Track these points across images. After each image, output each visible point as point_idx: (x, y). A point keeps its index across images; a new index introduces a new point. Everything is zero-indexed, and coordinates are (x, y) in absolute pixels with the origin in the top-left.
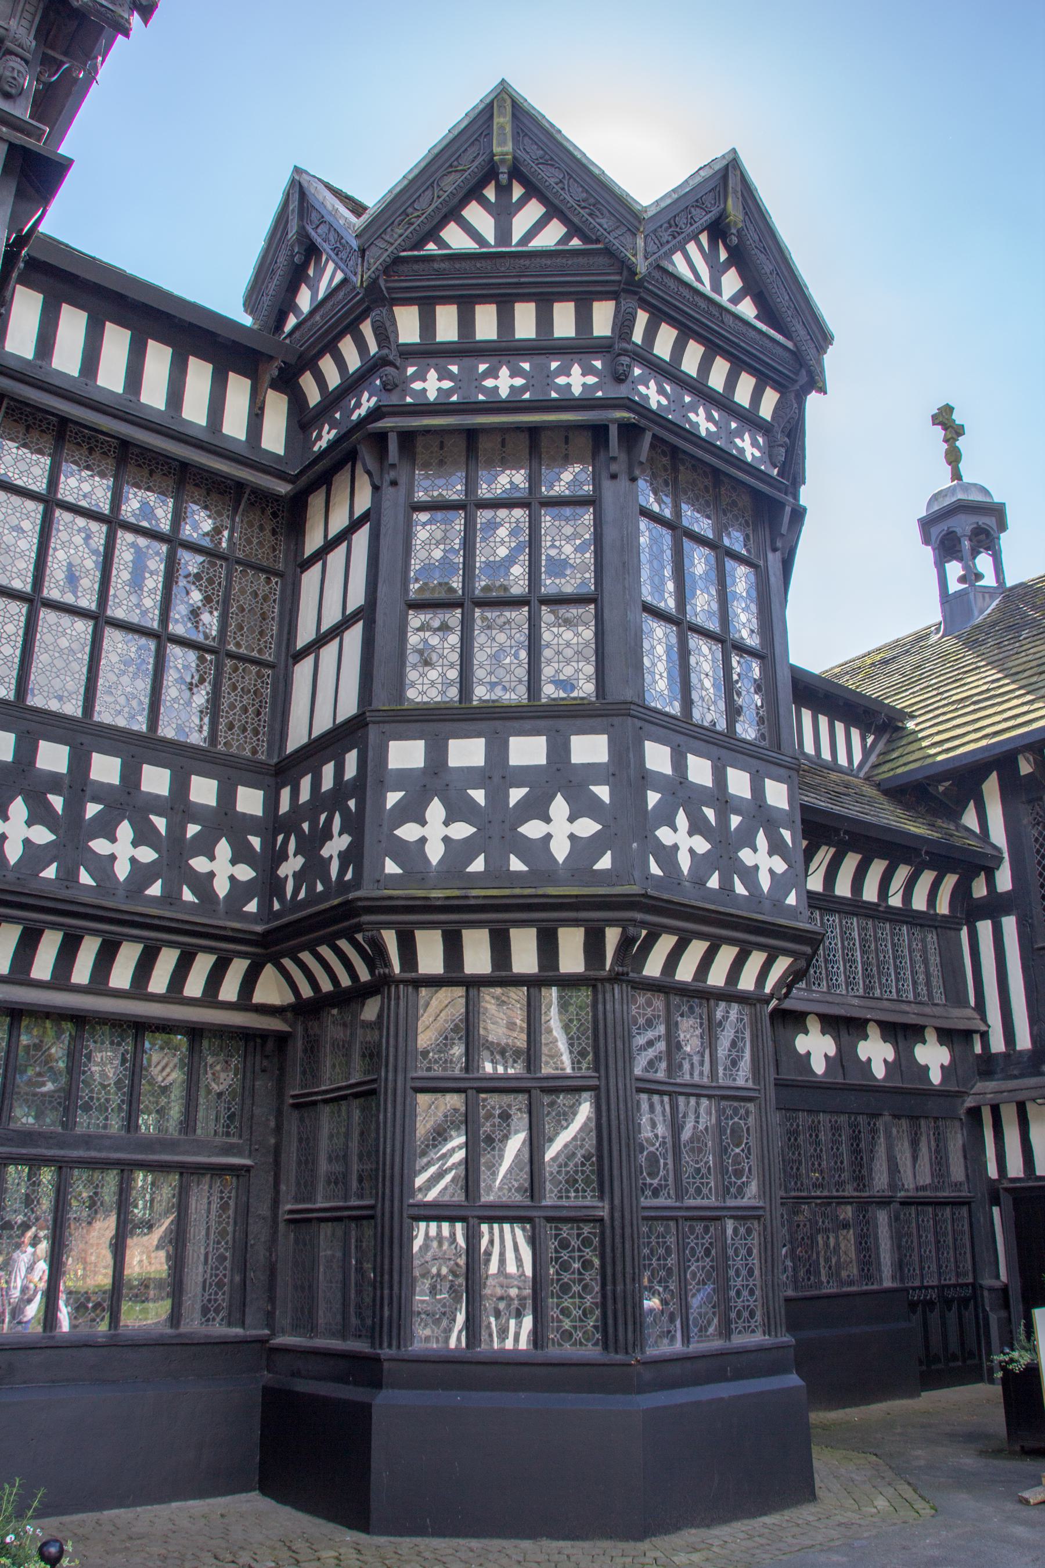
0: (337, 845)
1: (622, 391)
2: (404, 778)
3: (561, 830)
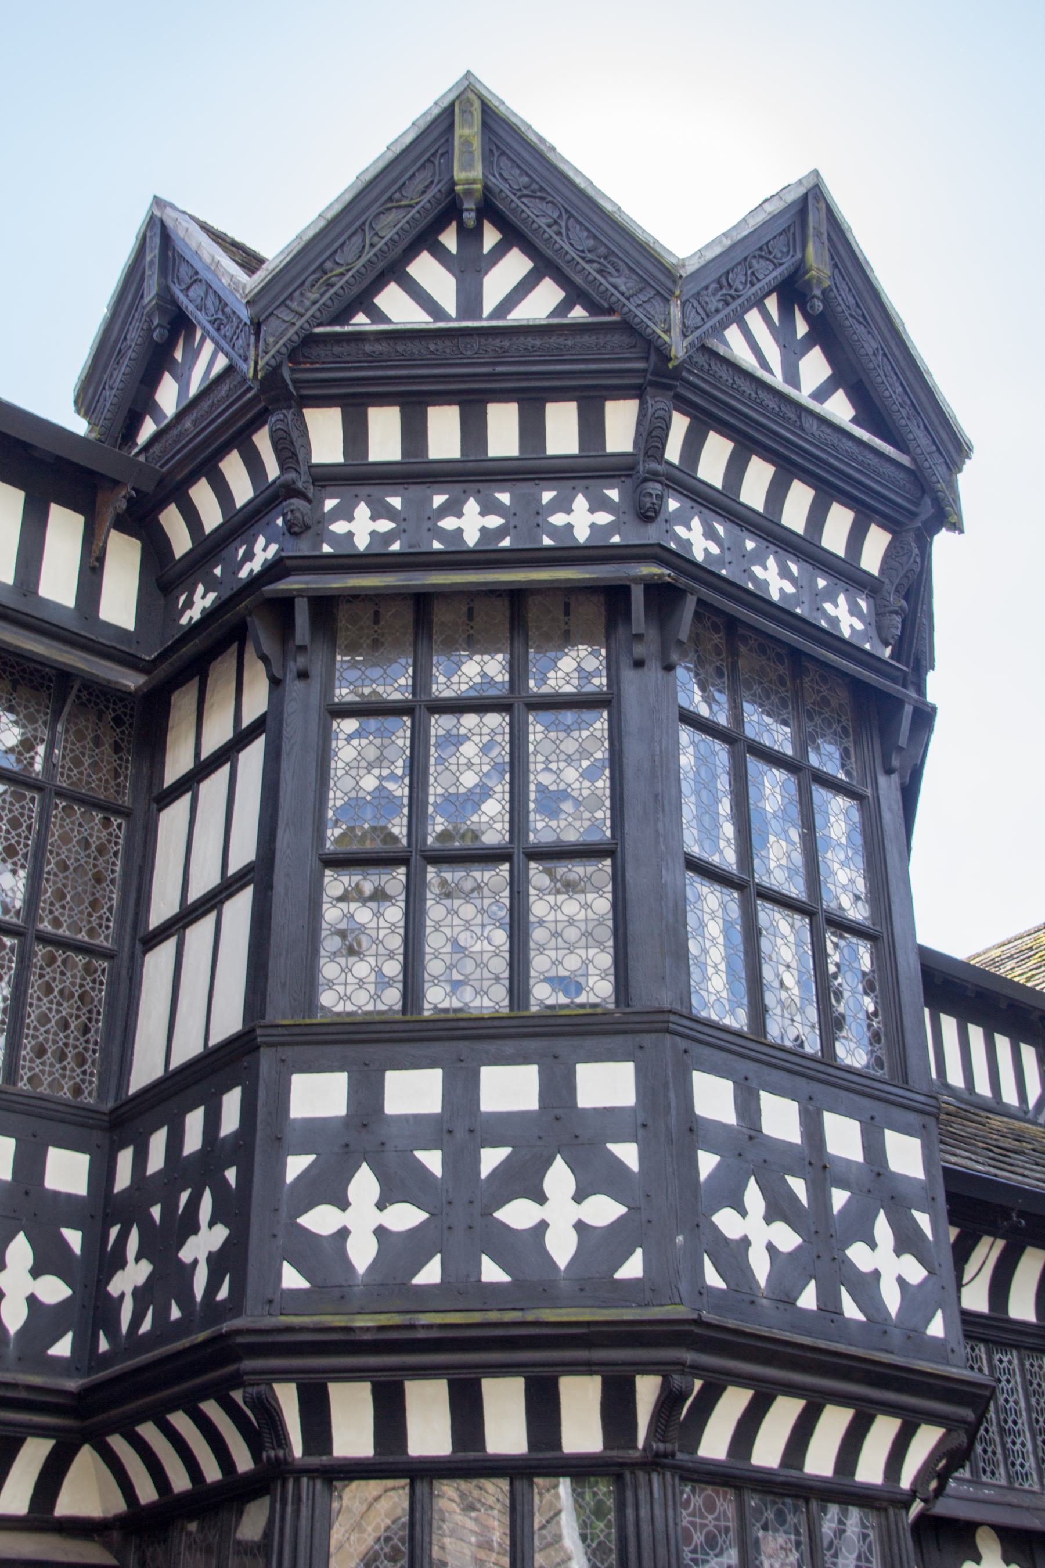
0: (205, 1242)
1: (651, 534)
2: (315, 1133)
3: (561, 1215)
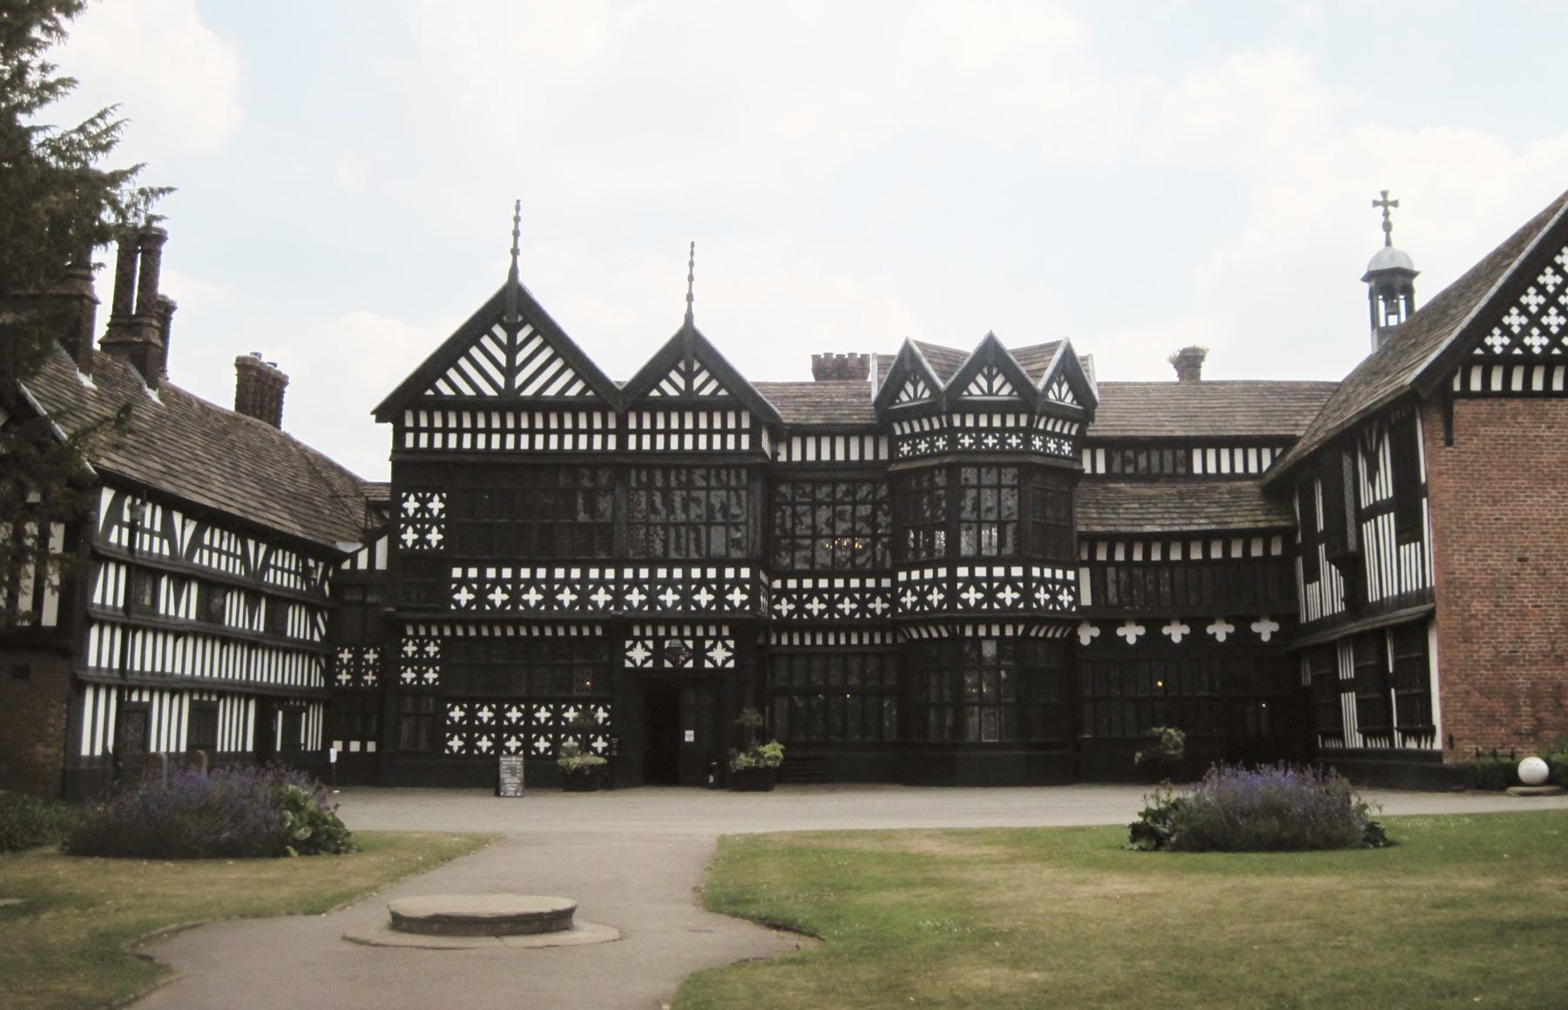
2: (962, 579)
3: (1008, 596)
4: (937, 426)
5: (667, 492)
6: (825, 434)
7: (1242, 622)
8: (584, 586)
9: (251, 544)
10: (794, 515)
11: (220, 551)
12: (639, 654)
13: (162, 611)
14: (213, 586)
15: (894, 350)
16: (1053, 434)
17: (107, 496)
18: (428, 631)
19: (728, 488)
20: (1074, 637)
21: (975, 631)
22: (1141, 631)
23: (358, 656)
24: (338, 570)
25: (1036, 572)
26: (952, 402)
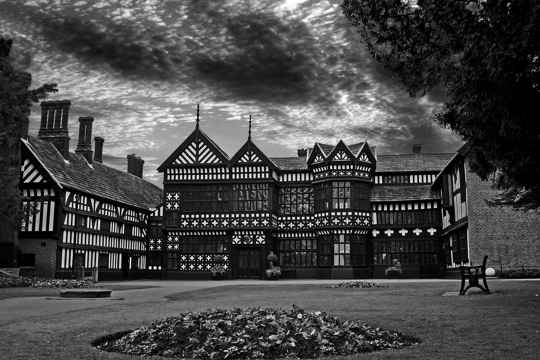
3: (347, 221)
4: (325, 169)
5: (244, 191)
6: (294, 173)
7: (424, 229)
8: (240, 220)
9: (119, 208)
10: (285, 197)
11: (108, 210)
12: (236, 240)
13: (88, 227)
14: (106, 221)
15: (312, 146)
16: (362, 171)
17: (68, 194)
18: (175, 234)
19: (262, 190)
20: (370, 234)
21: (337, 232)
22: (392, 232)
23: (156, 242)
24: (149, 216)
25: (356, 214)
26: (329, 162)
